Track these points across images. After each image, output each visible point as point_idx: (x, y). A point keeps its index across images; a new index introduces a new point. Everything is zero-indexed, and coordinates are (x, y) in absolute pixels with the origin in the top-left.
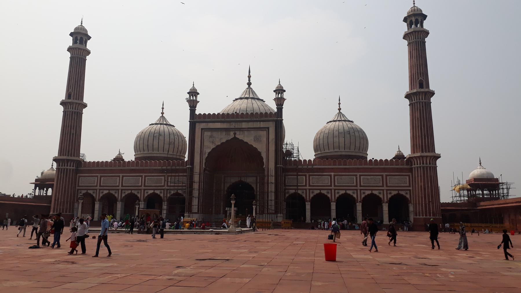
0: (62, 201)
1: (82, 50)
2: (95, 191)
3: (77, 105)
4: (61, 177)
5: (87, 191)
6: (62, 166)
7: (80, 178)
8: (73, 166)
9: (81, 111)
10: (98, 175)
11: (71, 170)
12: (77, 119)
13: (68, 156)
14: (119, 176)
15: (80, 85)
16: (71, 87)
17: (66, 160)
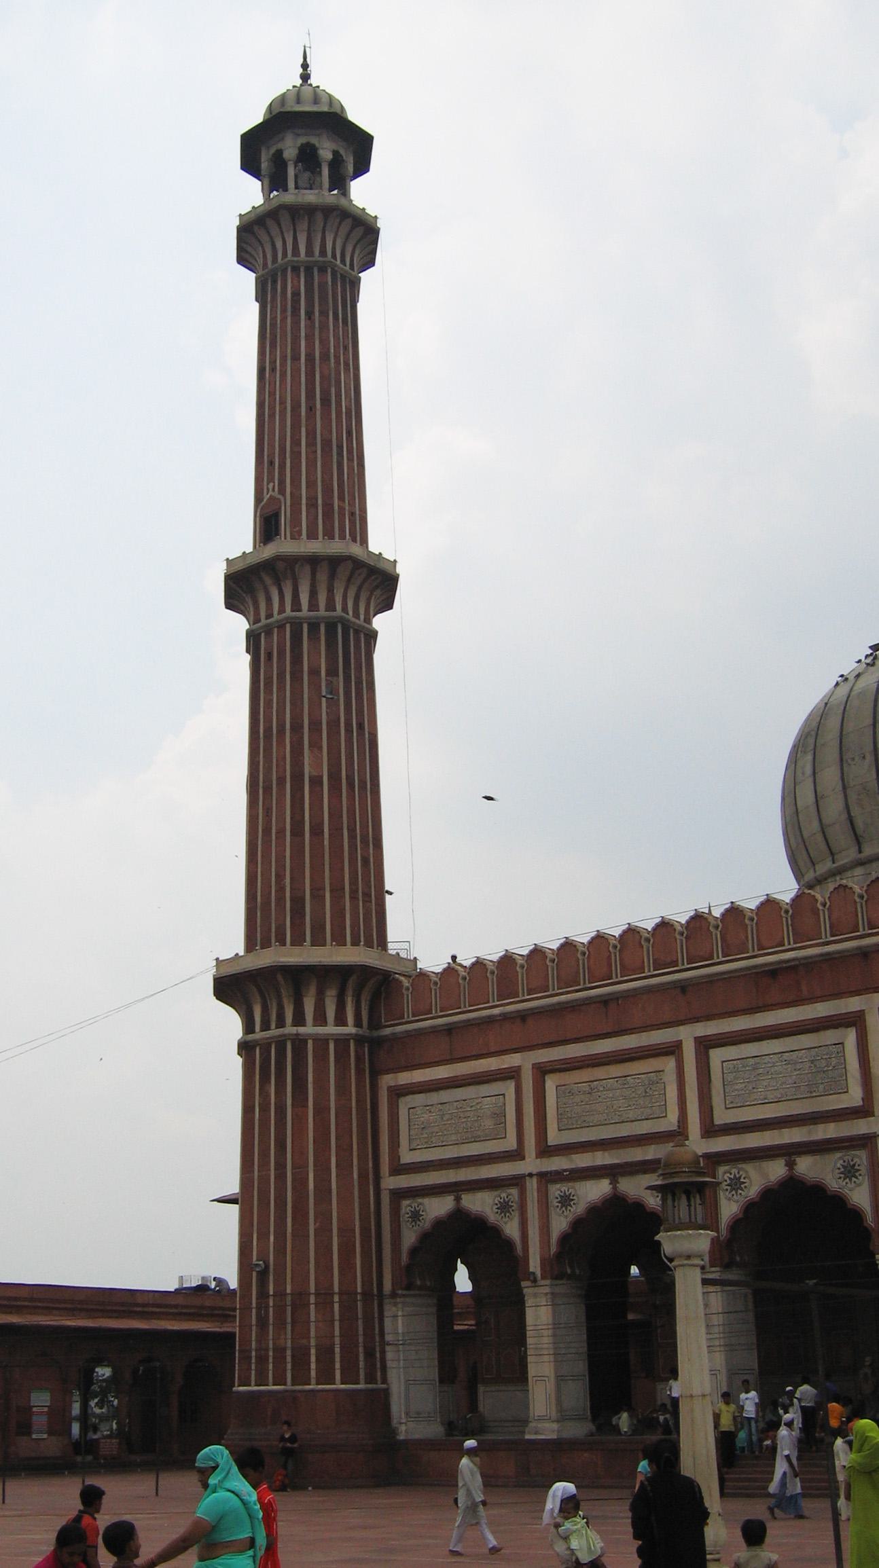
0: (289, 1291)
1: (319, 217)
2: (514, 1192)
3: (322, 577)
4: (265, 1108)
5: (458, 1199)
6: (266, 1026)
7: (405, 1103)
8: (340, 1020)
9: (357, 615)
10: (513, 1060)
11: (332, 1046)
12: (332, 672)
13: (298, 941)
14: (673, 1050)
15: (327, 443)
16: (271, 463)
17: (280, 977)
